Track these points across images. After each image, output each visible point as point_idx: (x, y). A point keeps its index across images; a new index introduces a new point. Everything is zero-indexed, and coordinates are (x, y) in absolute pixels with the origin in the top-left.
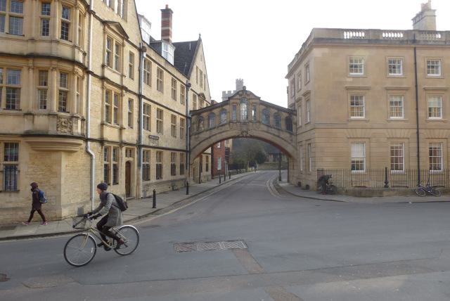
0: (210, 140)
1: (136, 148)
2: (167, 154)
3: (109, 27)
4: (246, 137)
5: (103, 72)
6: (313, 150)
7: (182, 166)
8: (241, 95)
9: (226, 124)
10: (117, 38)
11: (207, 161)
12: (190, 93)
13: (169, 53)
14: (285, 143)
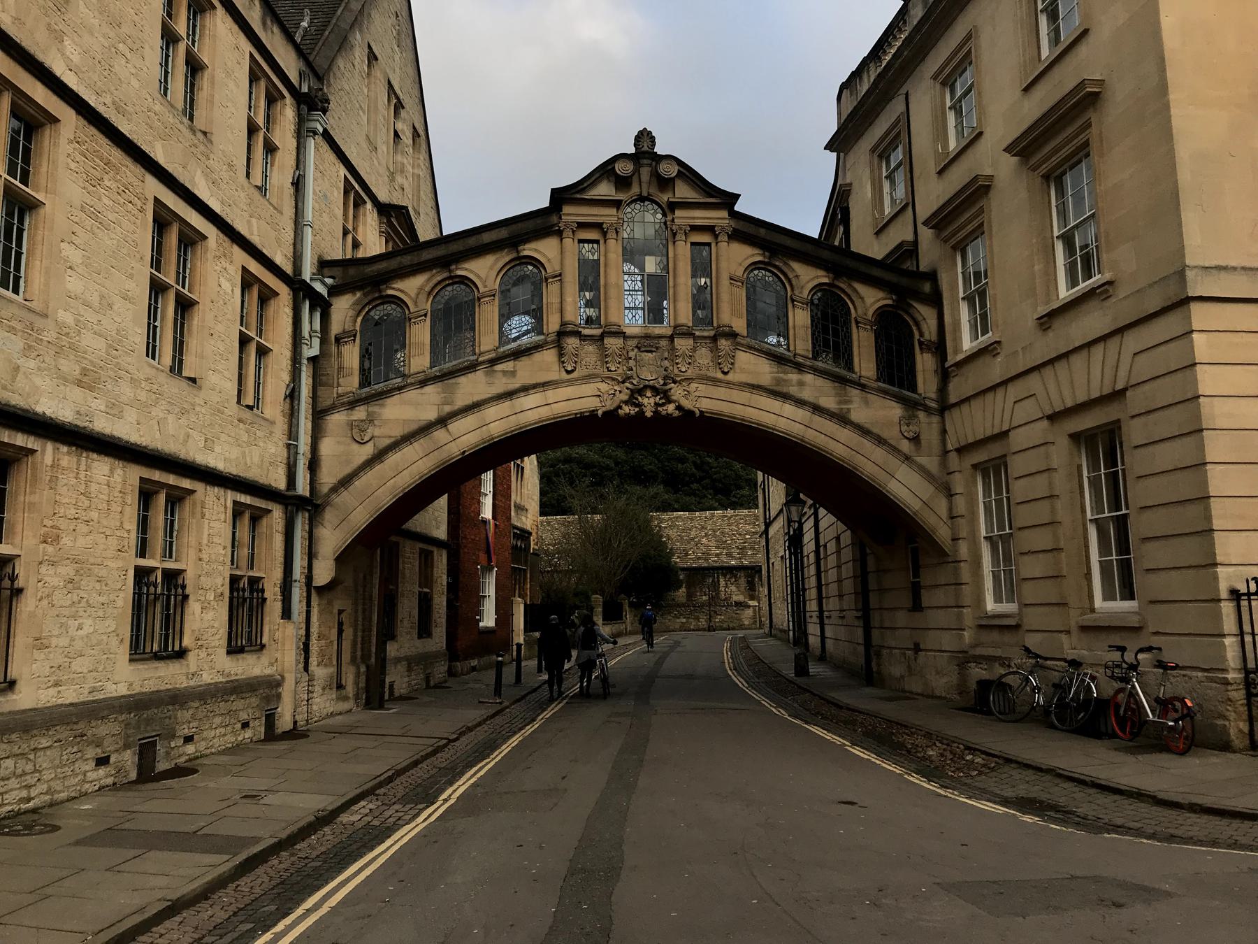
0: (440, 435)
11: (426, 578)
14: (879, 453)
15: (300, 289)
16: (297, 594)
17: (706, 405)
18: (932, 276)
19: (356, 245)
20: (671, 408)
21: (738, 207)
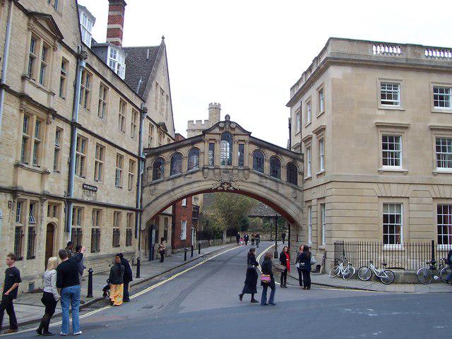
0: (172, 193)
1: (63, 203)
2: (107, 214)
3: (36, 21)
4: (228, 191)
5: (23, 87)
6: (328, 213)
7: (129, 233)
8: (223, 128)
9: (197, 171)
10: (45, 38)
11: (166, 226)
12: (146, 123)
13: (118, 61)
14: (285, 201)
15: (140, 159)
16: (138, 231)
17: (241, 188)
18: (303, 154)
19: (151, 138)
20: (231, 188)
21: (251, 135)
